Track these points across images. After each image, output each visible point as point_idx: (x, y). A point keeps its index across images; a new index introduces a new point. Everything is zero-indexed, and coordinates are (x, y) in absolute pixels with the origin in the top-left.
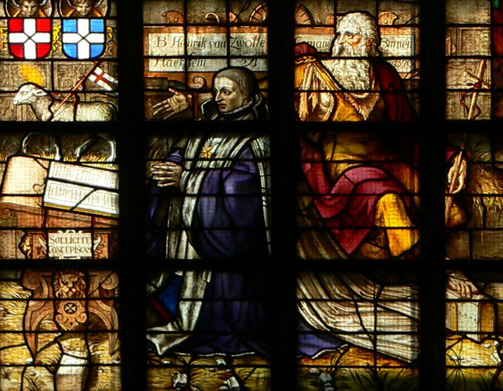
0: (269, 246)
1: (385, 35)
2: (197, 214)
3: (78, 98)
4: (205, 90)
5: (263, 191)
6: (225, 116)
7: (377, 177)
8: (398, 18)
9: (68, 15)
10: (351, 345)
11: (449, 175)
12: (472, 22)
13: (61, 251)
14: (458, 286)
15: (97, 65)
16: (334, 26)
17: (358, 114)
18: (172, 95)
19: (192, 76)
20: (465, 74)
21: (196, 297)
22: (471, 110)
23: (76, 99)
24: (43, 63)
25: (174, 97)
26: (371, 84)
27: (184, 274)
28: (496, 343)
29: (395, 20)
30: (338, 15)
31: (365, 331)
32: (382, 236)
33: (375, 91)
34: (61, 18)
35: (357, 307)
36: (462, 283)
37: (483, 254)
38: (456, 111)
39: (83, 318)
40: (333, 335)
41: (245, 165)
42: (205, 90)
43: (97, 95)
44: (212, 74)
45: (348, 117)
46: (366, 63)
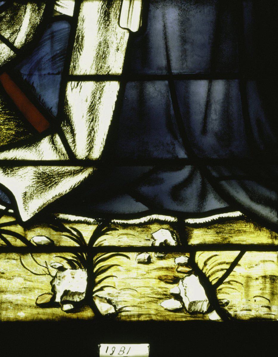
21: (103, 72)
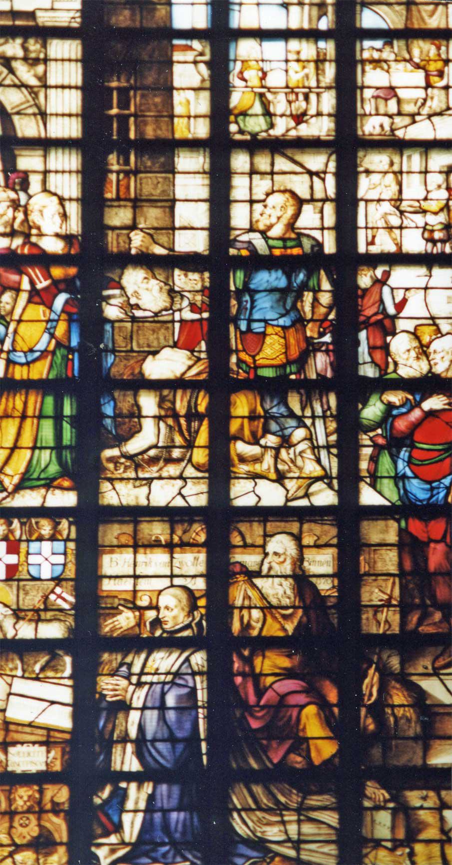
0: (205, 758)
1: (309, 555)
2: (141, 728)
3: (39, 616)
4: (149, 608)
5: (200, 704)
6: (168, 632)
7: (298, 689)
8: (319, 539)
9: (34, 538)
10: (277, 854)
11: (364, 687)
12: (384, 542)
13: (18, 765)
14: (375, 792)
15: (57, 585)
16: (263, 546)
17: (284, 629)
18: (120, 613)
19: (139, 594)
20: (377, 590)
22: (382, 625)
23: (37, 616)
24: (10, 583)
25: (124, 614)
26: (295, 600)
27: (128, 785)
28: (407, 850)
29: (316, 541)
30: (266, 536)
31: (289, 840)
32: (304, 746)
33: (299, 607)
34: (28, 541)
35: (282, 816)
36: (376, 791)
37: (395, 763)
38: (372, 625)
39: (35, 832)
40: (260, 844)
41: (183, 679)
42: (149, 608)
43: (57, 613)
44: (157, 593)
45: (276, 631)
46: (291, 580)
